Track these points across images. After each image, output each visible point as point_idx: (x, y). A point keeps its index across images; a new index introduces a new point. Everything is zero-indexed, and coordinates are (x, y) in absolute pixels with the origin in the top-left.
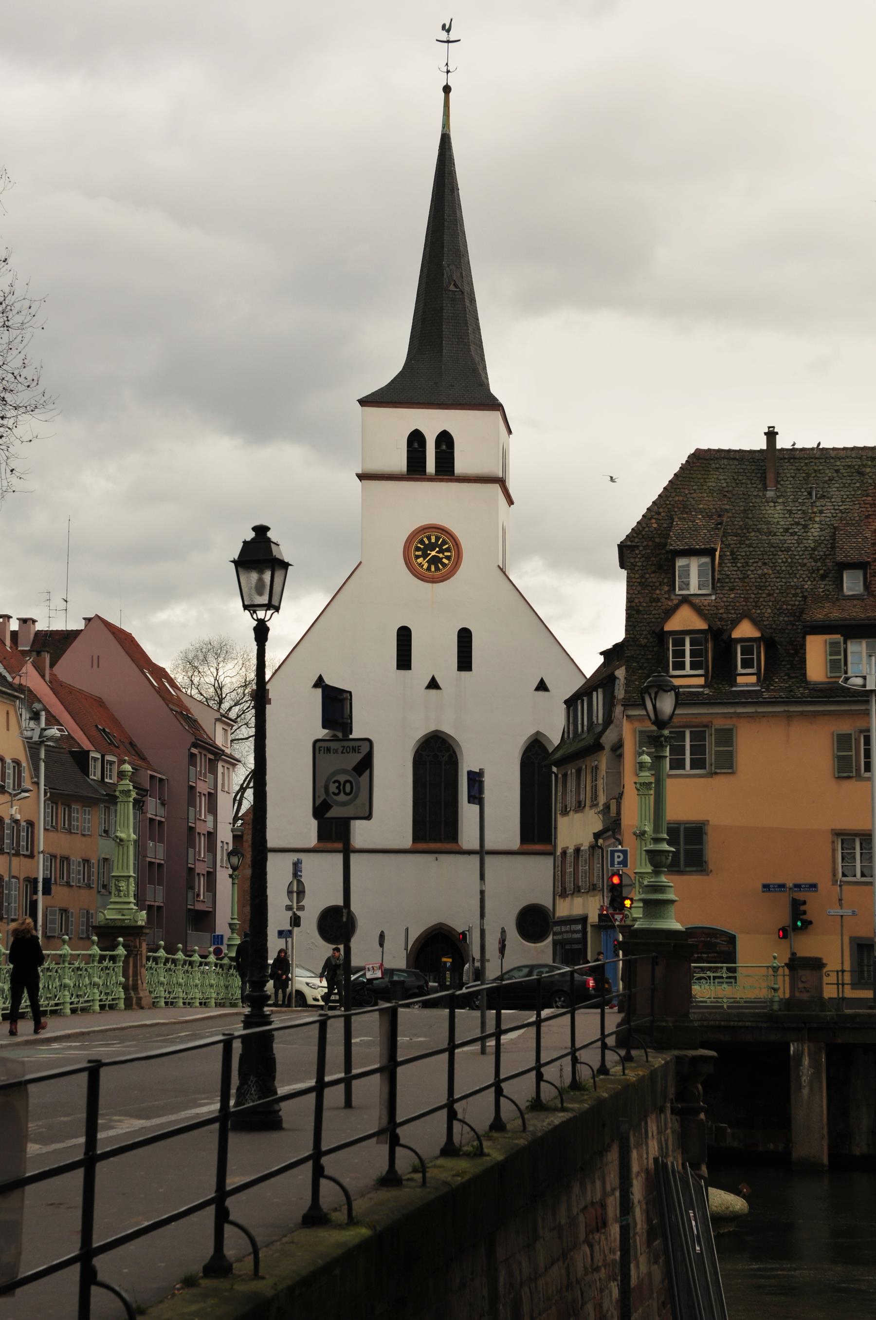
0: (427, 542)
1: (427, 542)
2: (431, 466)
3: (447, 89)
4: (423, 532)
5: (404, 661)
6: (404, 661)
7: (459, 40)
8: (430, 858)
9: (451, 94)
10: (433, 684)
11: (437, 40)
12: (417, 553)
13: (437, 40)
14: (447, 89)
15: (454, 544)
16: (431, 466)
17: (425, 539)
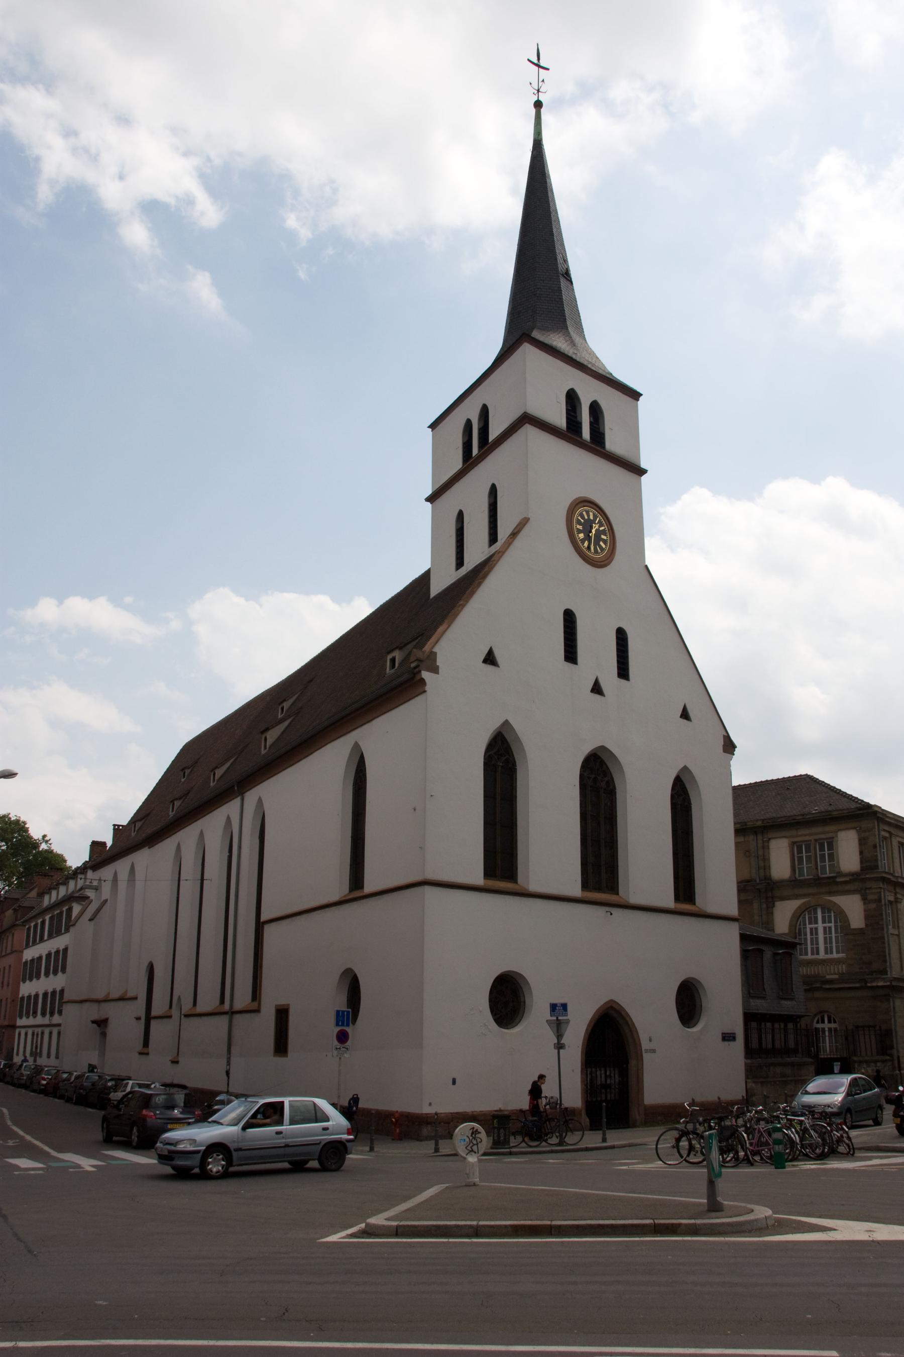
0: (586, 517)
1: (586, 517)
2: (586, 434)
3: (538, 105)
4: (582, 504)
5: (571, 655)
6: (571, 655)
7: (548, 69)
8: (600, 911)
9: (542, 110)
10: (597, 689)
11: (529, 60)
12: (578, 527)
13: (529, 60)
14: (538, 105)
15: (610, 528)
16: (586, 434)
17: (584, 513)
